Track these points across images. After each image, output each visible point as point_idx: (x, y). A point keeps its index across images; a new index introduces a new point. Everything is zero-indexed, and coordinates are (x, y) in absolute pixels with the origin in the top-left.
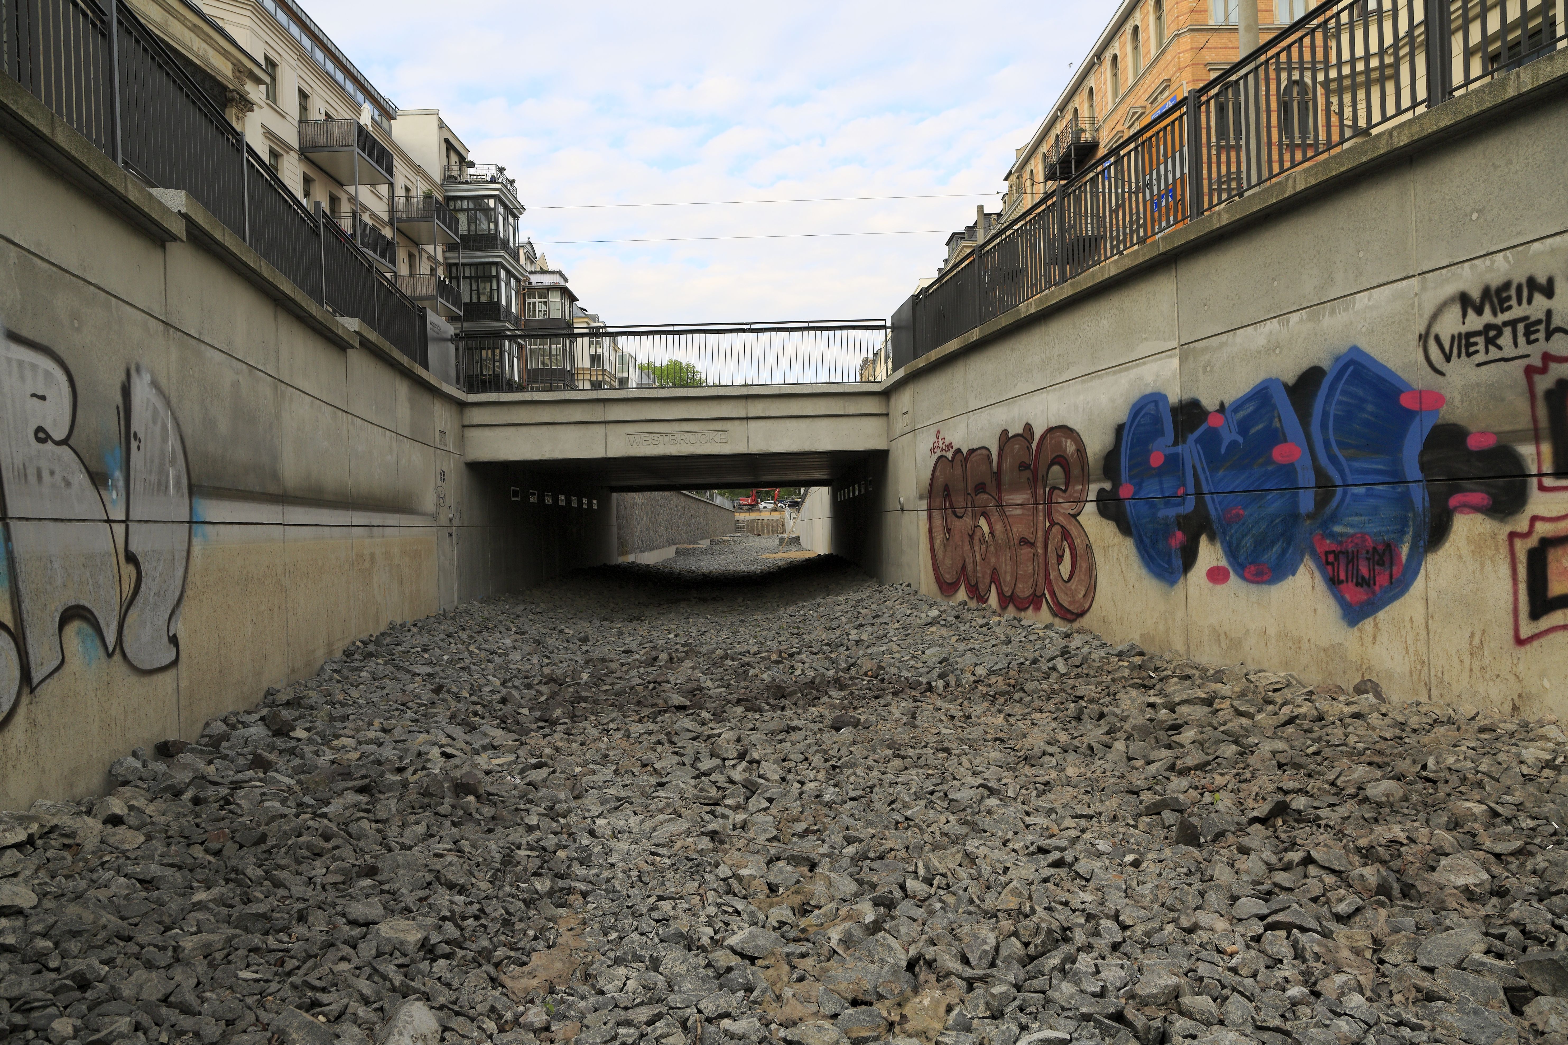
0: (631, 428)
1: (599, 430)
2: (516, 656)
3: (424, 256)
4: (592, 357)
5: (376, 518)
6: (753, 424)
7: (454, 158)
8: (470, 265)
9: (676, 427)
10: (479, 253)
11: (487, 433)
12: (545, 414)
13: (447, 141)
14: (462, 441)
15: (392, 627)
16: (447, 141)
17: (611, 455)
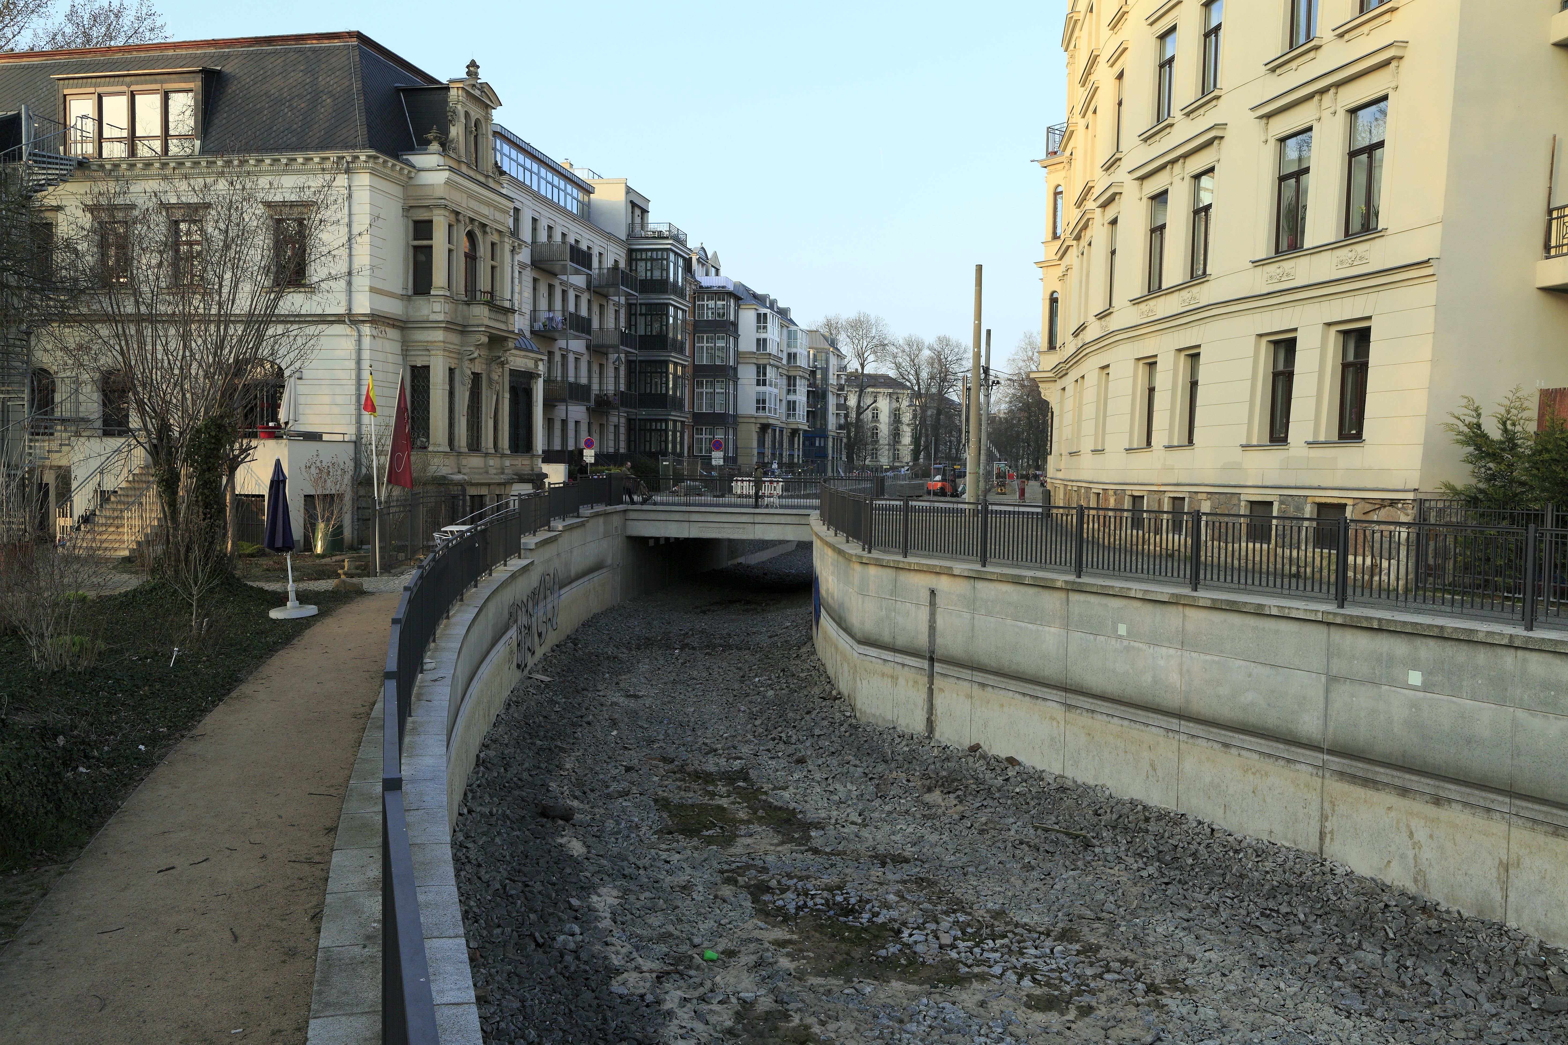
0: (701, 525)
1: (686, 524)
2: (637, 629)
3: (611, 303)
4: (758, 340)
5: (591, 576)
6: (757, 526)
7: (638, 212)
8: (646, 304)
9: (721, 525)
10: (653, 296)
11: (636, 523)
12: (663, 516)
13: (631, 202)
14: (624, 526)
15: (595, 615)
16: (631, 202)
17: (692, 536)
